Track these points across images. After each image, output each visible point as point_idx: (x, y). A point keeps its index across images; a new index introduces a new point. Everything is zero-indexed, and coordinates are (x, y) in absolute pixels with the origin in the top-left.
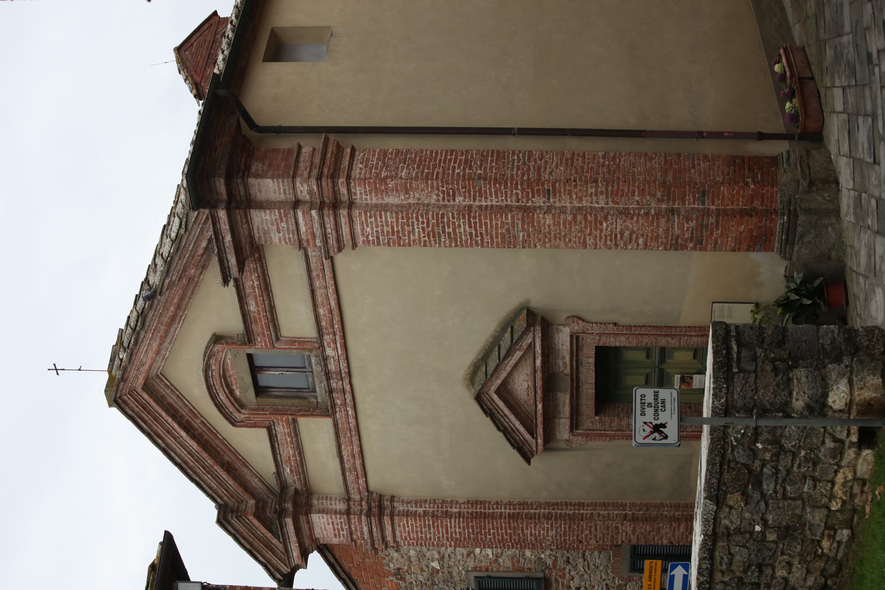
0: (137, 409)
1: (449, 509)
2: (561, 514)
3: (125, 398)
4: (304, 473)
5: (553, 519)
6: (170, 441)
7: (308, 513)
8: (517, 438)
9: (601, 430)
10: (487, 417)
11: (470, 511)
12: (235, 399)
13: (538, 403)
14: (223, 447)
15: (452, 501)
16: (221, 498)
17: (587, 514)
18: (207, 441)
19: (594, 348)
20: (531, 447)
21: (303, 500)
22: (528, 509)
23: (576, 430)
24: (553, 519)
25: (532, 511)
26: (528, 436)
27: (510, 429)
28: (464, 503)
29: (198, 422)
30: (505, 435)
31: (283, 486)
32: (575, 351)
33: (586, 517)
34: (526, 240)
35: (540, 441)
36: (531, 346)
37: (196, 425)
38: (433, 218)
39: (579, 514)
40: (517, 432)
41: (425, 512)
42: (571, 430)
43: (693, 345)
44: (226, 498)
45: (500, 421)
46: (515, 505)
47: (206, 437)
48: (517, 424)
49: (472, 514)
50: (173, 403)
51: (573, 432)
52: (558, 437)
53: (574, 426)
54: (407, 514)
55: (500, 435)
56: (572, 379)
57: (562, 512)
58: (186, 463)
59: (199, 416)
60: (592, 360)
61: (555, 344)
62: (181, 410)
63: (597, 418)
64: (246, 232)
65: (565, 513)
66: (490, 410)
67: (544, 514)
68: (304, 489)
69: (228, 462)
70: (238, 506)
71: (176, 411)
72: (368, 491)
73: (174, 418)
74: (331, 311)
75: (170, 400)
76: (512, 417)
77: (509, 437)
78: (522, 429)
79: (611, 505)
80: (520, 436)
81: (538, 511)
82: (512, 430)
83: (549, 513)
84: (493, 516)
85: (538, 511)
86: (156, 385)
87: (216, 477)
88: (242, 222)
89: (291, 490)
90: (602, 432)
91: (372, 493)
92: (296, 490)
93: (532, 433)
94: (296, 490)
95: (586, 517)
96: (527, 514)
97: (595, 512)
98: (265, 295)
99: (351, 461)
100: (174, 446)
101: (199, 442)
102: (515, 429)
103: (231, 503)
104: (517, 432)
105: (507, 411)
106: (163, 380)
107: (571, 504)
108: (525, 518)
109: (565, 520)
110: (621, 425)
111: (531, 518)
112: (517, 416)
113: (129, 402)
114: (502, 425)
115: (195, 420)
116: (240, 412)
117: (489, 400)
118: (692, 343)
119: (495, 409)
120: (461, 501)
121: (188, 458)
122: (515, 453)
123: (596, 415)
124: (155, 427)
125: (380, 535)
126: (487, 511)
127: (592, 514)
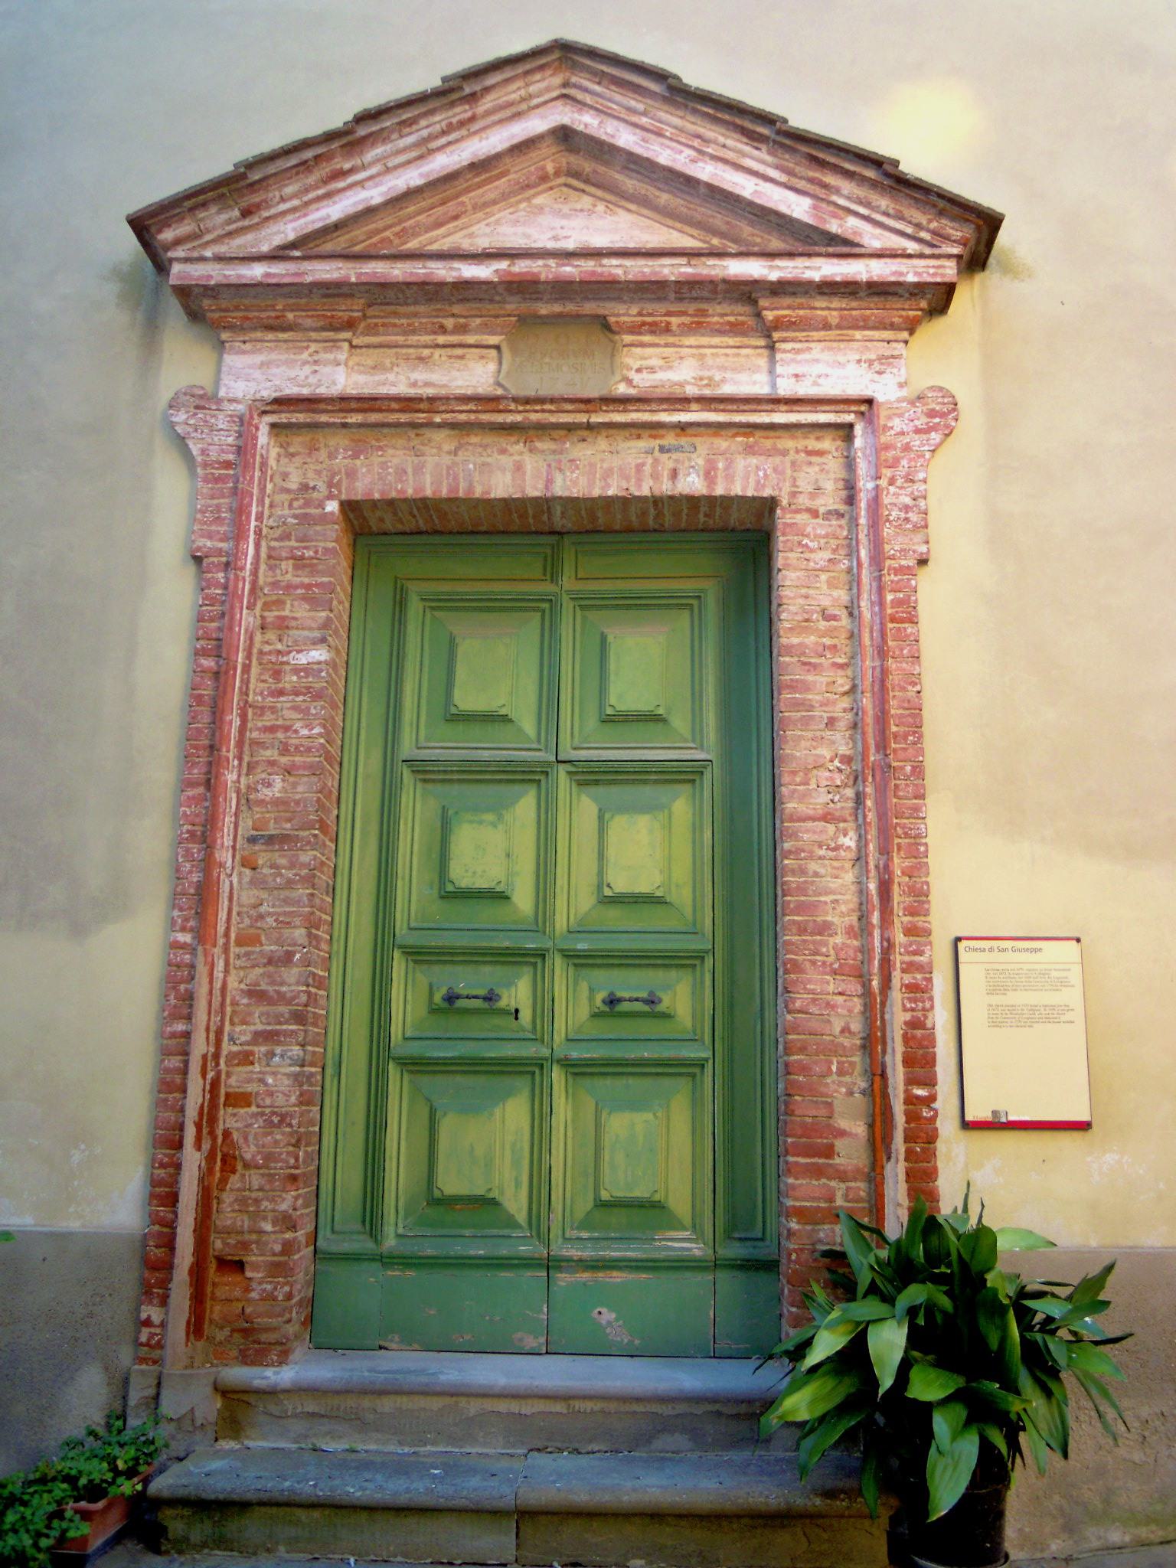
8: (289, 190)
9: (260, 517)
10: (444, 79)
13: (503, 265)
19: (767, 492)
26: (288, 230)
27: (347, 166)
30: (330, 137)
35: (257, 271)
36: (844, 247)
40: (320, 192)
42: (282, 403)
43: (803, 872)
48: (375, 194)
53: (283, 418)
60: (692, 484)
61: (798, 352)
63: (332, 507)
66: (473, 98)
76: (412, 177)
77: (309, 154)
78: (335, 210)
80: (296, 202)
82: (341, 174)
90: (253, 524)
93: (306, 246)
102: (341, 184)
104: (320, 192)
105: (443, 162)
117: (523, 100)
118: (813, 866)
119: (473, 119)
123: (350, 507)
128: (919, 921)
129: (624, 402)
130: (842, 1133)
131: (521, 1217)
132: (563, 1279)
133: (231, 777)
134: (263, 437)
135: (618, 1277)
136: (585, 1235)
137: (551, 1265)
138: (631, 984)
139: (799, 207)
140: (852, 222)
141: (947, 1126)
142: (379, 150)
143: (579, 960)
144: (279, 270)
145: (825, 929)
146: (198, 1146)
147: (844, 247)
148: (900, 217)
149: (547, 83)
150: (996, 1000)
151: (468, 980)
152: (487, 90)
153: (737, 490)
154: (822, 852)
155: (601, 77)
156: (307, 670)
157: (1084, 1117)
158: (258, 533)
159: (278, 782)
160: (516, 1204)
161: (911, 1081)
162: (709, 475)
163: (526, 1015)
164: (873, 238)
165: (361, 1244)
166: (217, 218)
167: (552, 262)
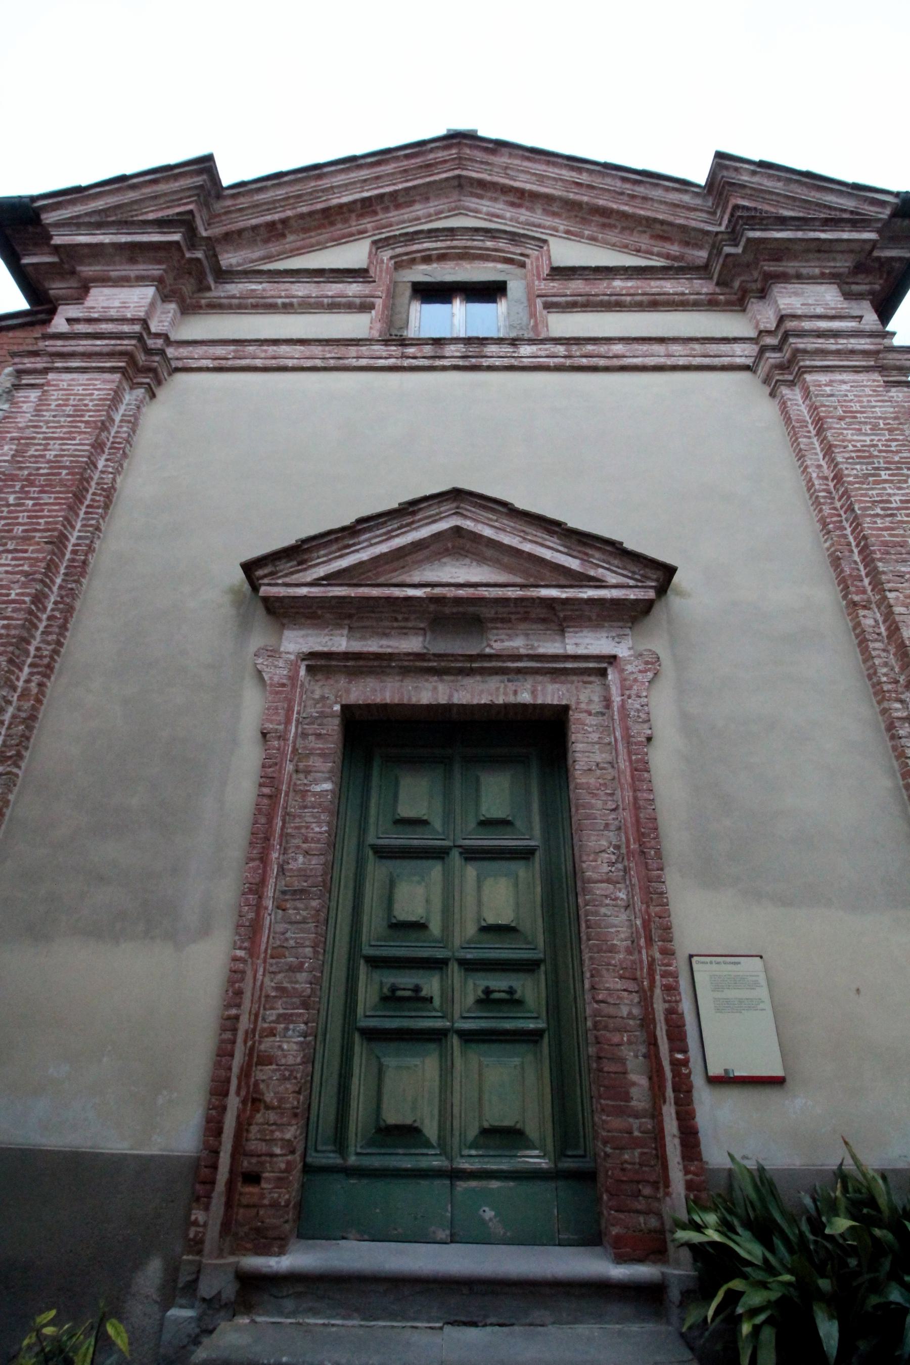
0: (432, 156)
1: (105, 456)
2: (37, 628)
3: (454, 151)
4: (240, 307)
5: (33, 607)
6: (364, 173)
7: (159, 282)
8: (322, 552)
9: (298, 713)
10: (400, 504)
11: (93, 484)
12: (413, 261)
13: (428, 590)
14: (313, 240)
15: (121, 465)
16: (233, 196)
17: (18, 679)
18: (332, 224)
19: (564, 702)
20: (286, 576)
21: (187, 287)
22: (66, 574)
23: (309, 669)
24: (33, 607)
25: (58, 581)
26: (321, 571)
27: (351, 542)
28: (114, 480)
29: (369, 226)
30: (343, 529)
31: (224, 275)
32: (561, 665)
33: (13, 673)
34: (902, 577)
35: (304, 591)
36: (599, 583)
37: (365, 221)
38: (901, 458)
39: (24, 662)
40: (337, 554)
41: (113, 421)
42: (313, 655)
43: (596, 913)
44: (229, 202)
45: (378, 526)
46: (86, 555)
47: (339, 226)
48: (364, 556)
49: (88, 483)
50: (411, 209)
51: (303, 660)
52: (288, 634)
54: (116, 399)
55: (347, 520)
56: (471, 658)
57: (39, 633)
58: (319, 177)
59: (377, 232)
60: (525, 697)
61: (576, 632)
62: (396, 213)
63: (337, 708)
64: (804, 271)
65: (33, 637)
66: (414, 513)
67: (46, 597)
68: (203, 302)
69: (283, 236)
70: (208, 208)
71: (398, 206)
72: (177, 370)
73: (394, 195)
74: (616, 356)
75: (417, 206)
76: (384, 548)
77: (333, 537)
78: (344, 563)
79: (27, 733)
80: (325, 559)
81: (55, 589)
82: (349, 546)
83: (45, 608)
84: (73, 509)
85: (55, 589)
86: (446, 201)
87: (272, 205)
88: (824, 267)
89: (211, 280)
90: (295, 716)
91: (170, 374)
92: (209, 289)
94: (209, 289)
95: (13, 673)
96: (57, 567)
97: (16, 696)
98: (645, 298)
99: (263, 355)
100: (353, 175)
101: (341, 206)
102: (348, 551)
103: (219, 206)
104: (337, 554)
106: (449, 211)
107: (56, 652)
108: (51, 560)
109: (23, 626)
110: (308, 756)
111: (48, 568)
112: (377, 560)
113: (446, 153)
114: (369, 529)
115: (372, 224)
116: (391, 258)
117: (438, 514)
119: (413, 523)
120: (119, 479)
121: (325, 183)
122: (289, 540)
123: (345, 707)
124: (394, 165)
125: (80, 349)
126: (84, 509)
127: (14, 689)
128: (668, 945)
129: (490, 657)
130: (634, 1084)
131: (434, 1139)
132: (461, 1185)
133: (275, 855)
134: (303, 672)
135: (495, 1184)
136: (473, 1152)
137: (456, 1175)
138: (499, 983)
139: (574, 564)
140: (600, 570)
141: (698, 1080)
142: (367, 536)
143: (470, 966)
144: (316, 591)
145: (612, 949)
146: (238, 1093)
147: (599, 583)
148: (625, 569)
149: (447, 507)
150: (718, 995)
151: (406, 980)
152: (420, 509)
153: (549, 701)
154: (608, 901)
155: (475, 505)
156: (321, 794)
157: (778, 1072)
158: (297, 721)
159: (301, 859)
160: (431, 1130)
161: (672, 1050)
162: (534, 693)
163: (437, 1002)
164: (612, 579)
165: (334, 1159)
166: (285, 566)
167: (452, 589)
